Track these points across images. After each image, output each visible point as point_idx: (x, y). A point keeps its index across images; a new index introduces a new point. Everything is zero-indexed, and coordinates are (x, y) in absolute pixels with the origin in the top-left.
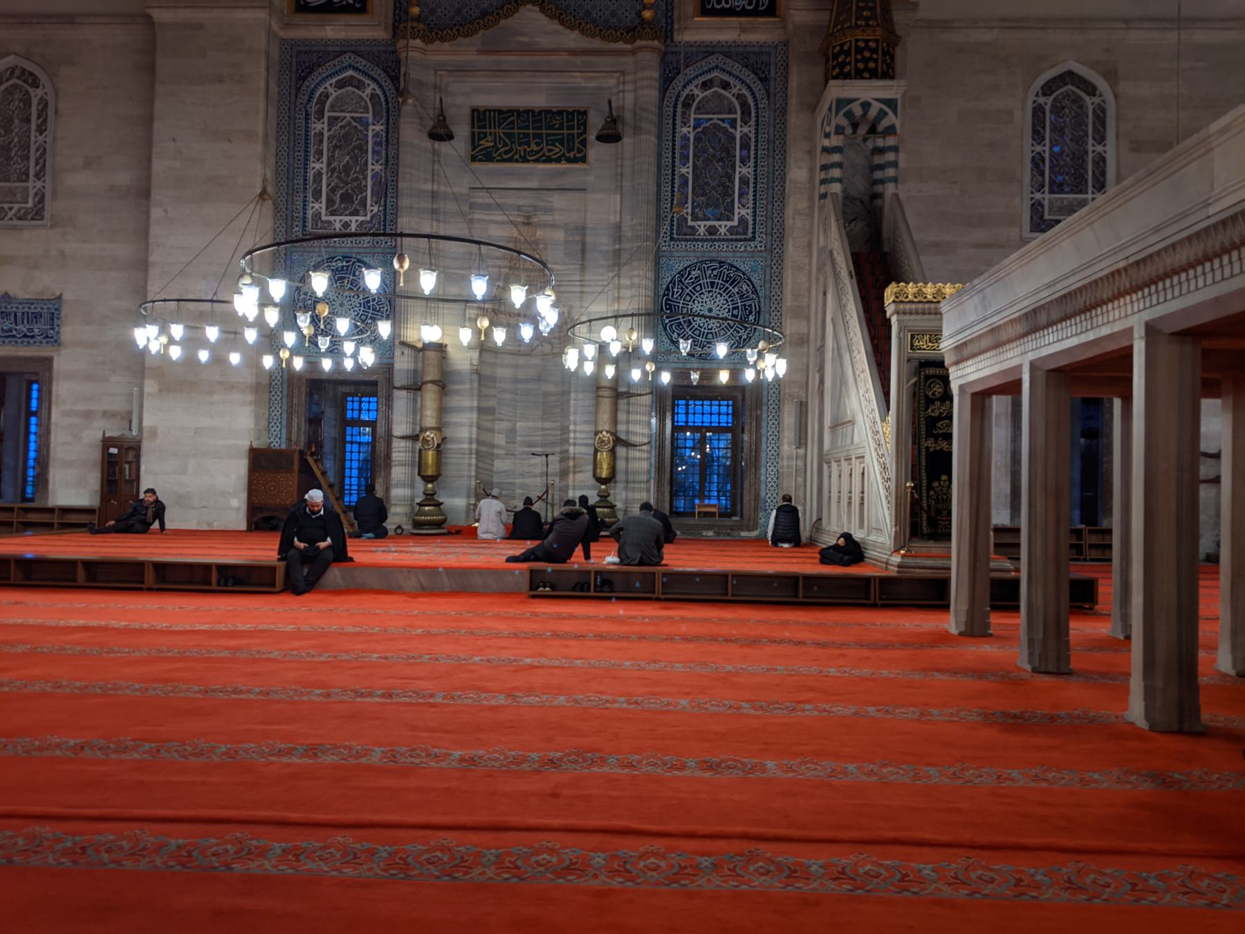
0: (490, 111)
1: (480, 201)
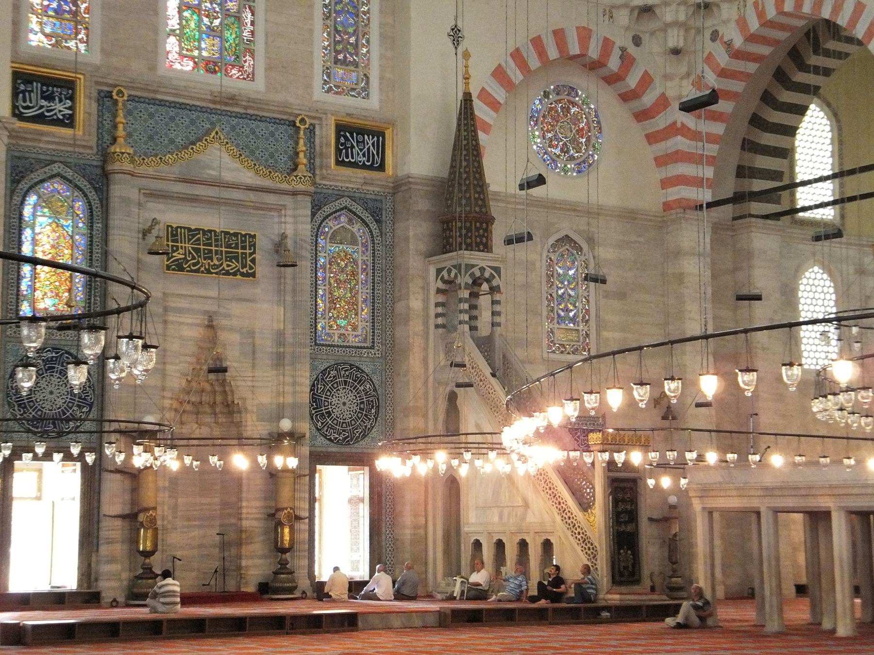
0: (181, 228)
1: (173, 305)
